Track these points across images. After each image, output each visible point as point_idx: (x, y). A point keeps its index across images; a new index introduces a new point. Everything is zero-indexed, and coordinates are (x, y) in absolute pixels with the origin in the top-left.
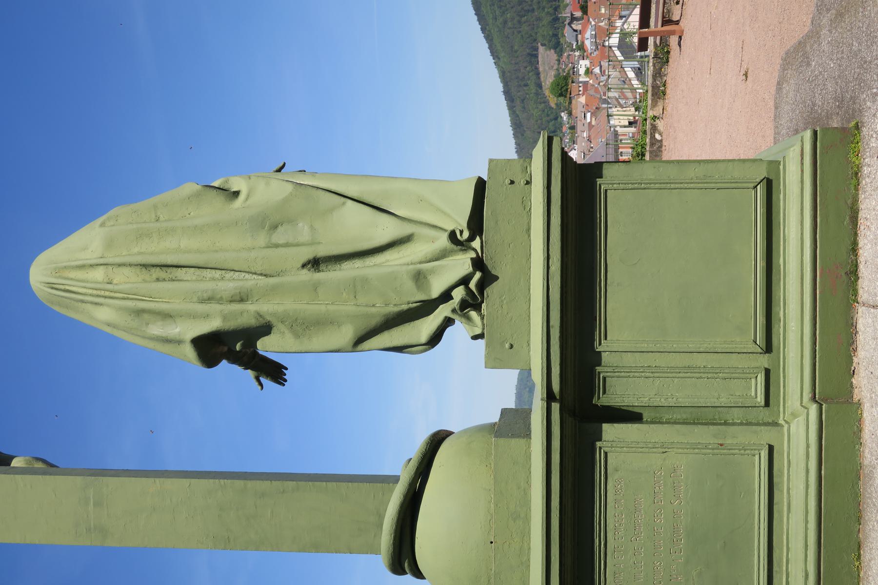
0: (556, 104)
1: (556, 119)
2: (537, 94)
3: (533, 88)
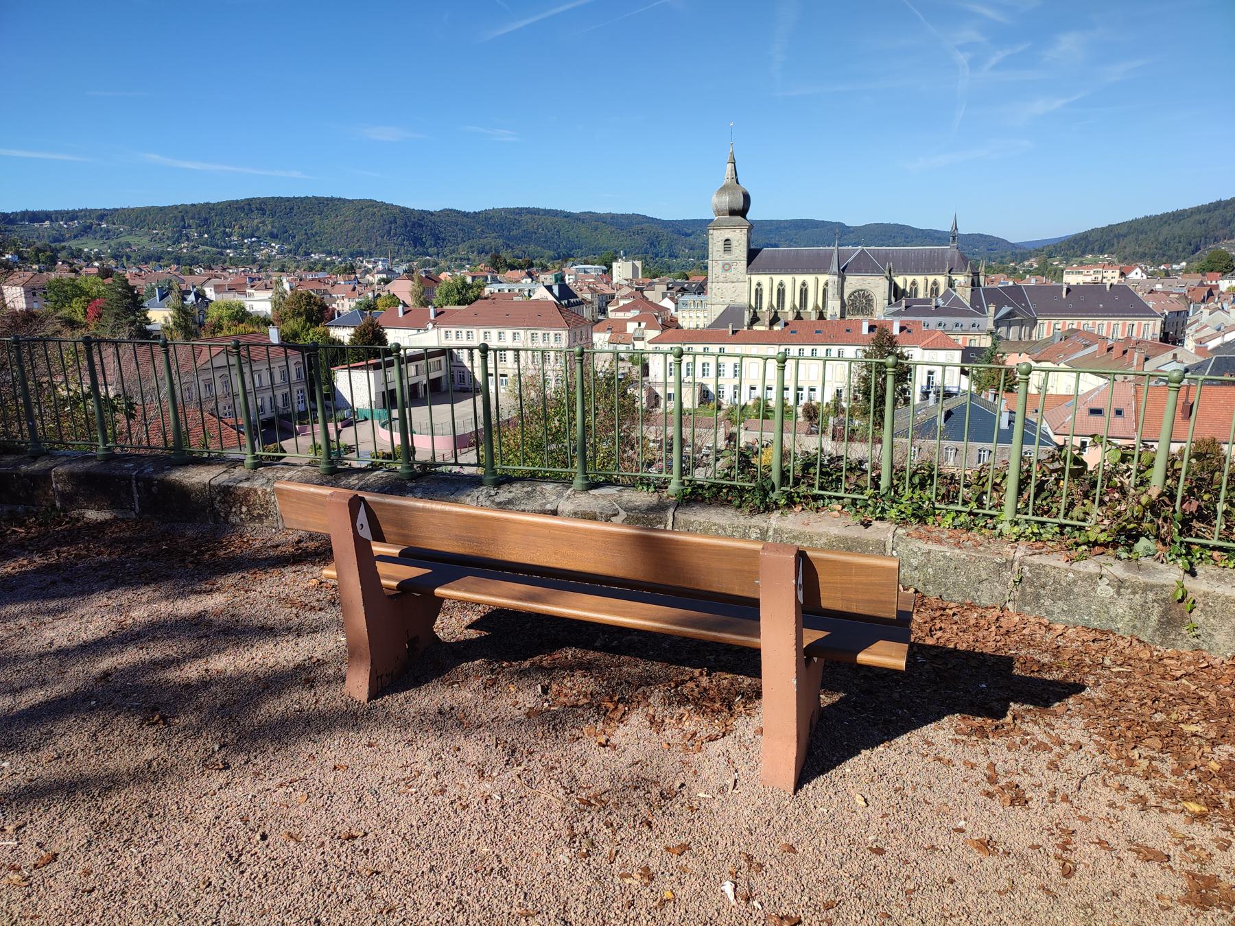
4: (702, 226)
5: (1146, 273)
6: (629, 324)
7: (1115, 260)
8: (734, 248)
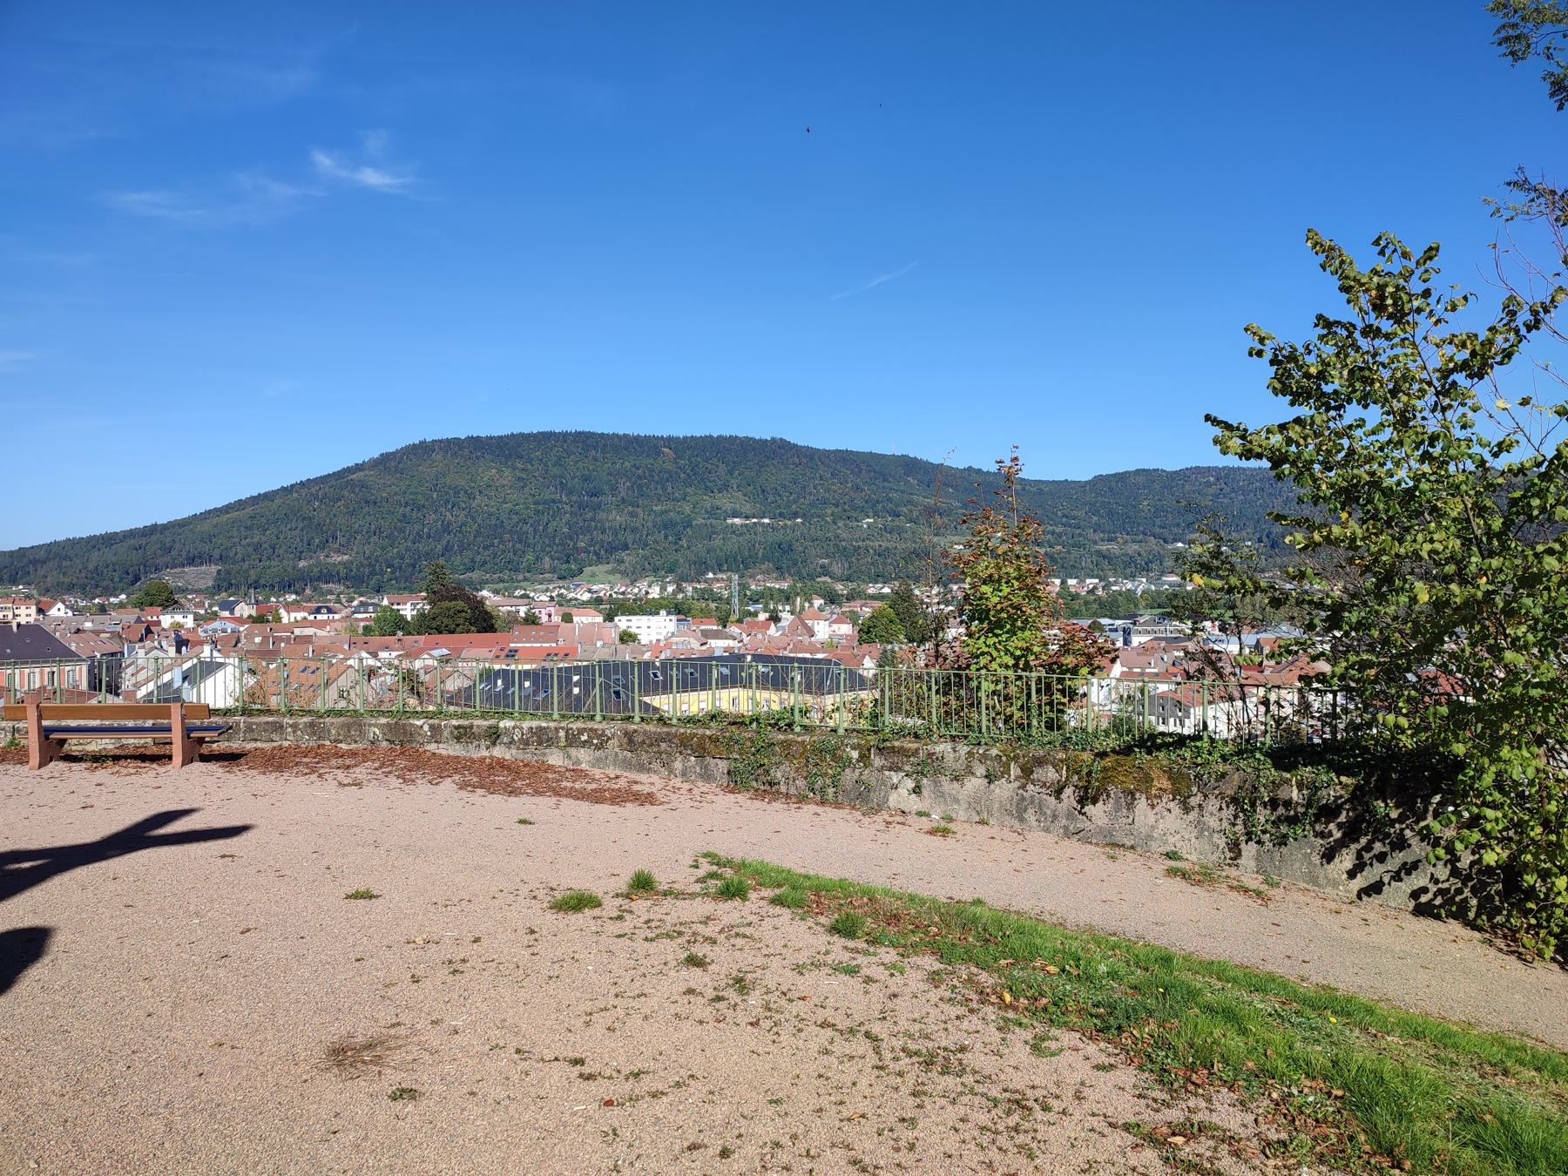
5: (71, 608)
7: (35, 592)
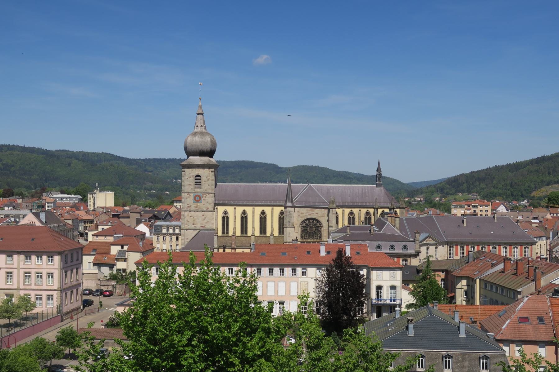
0: (534, 197)
1: (522, 196)
2: (542, 182)
3: (547, 179)
4: (180, 166)
6: (112, 247)
8: (203, 183)
